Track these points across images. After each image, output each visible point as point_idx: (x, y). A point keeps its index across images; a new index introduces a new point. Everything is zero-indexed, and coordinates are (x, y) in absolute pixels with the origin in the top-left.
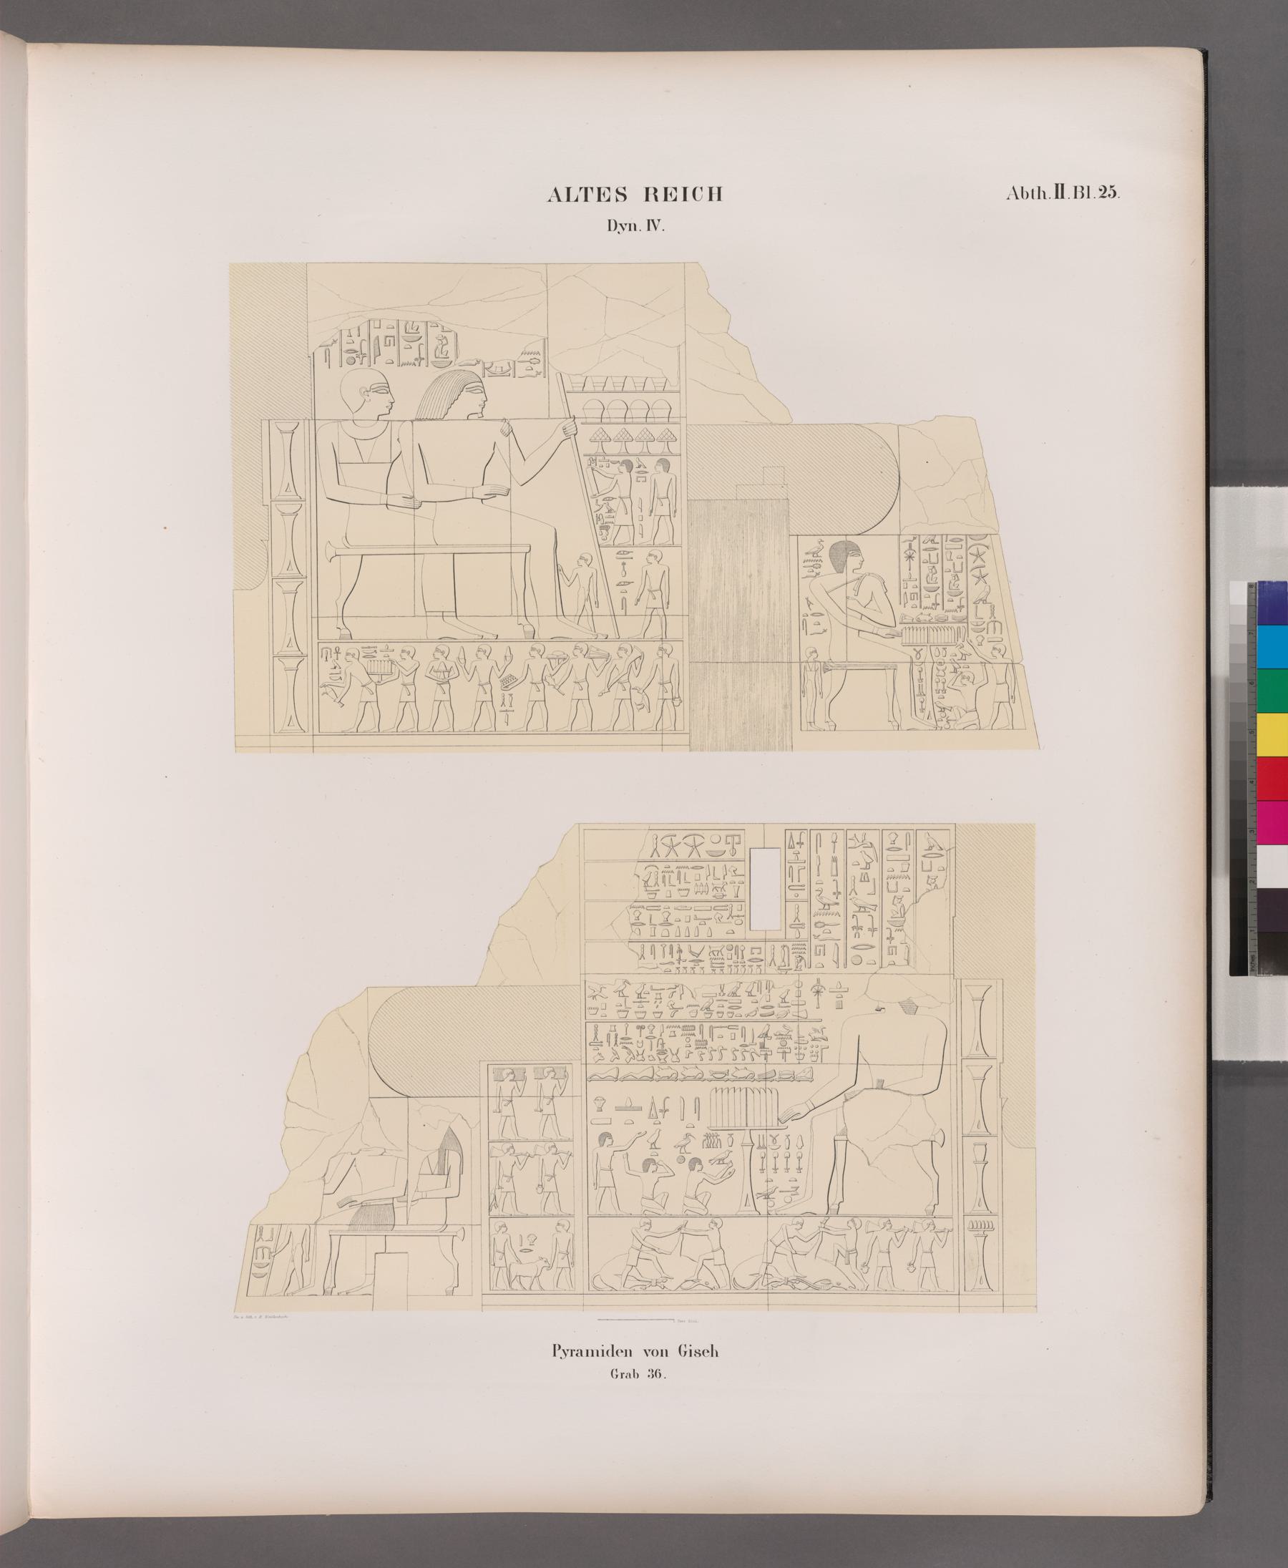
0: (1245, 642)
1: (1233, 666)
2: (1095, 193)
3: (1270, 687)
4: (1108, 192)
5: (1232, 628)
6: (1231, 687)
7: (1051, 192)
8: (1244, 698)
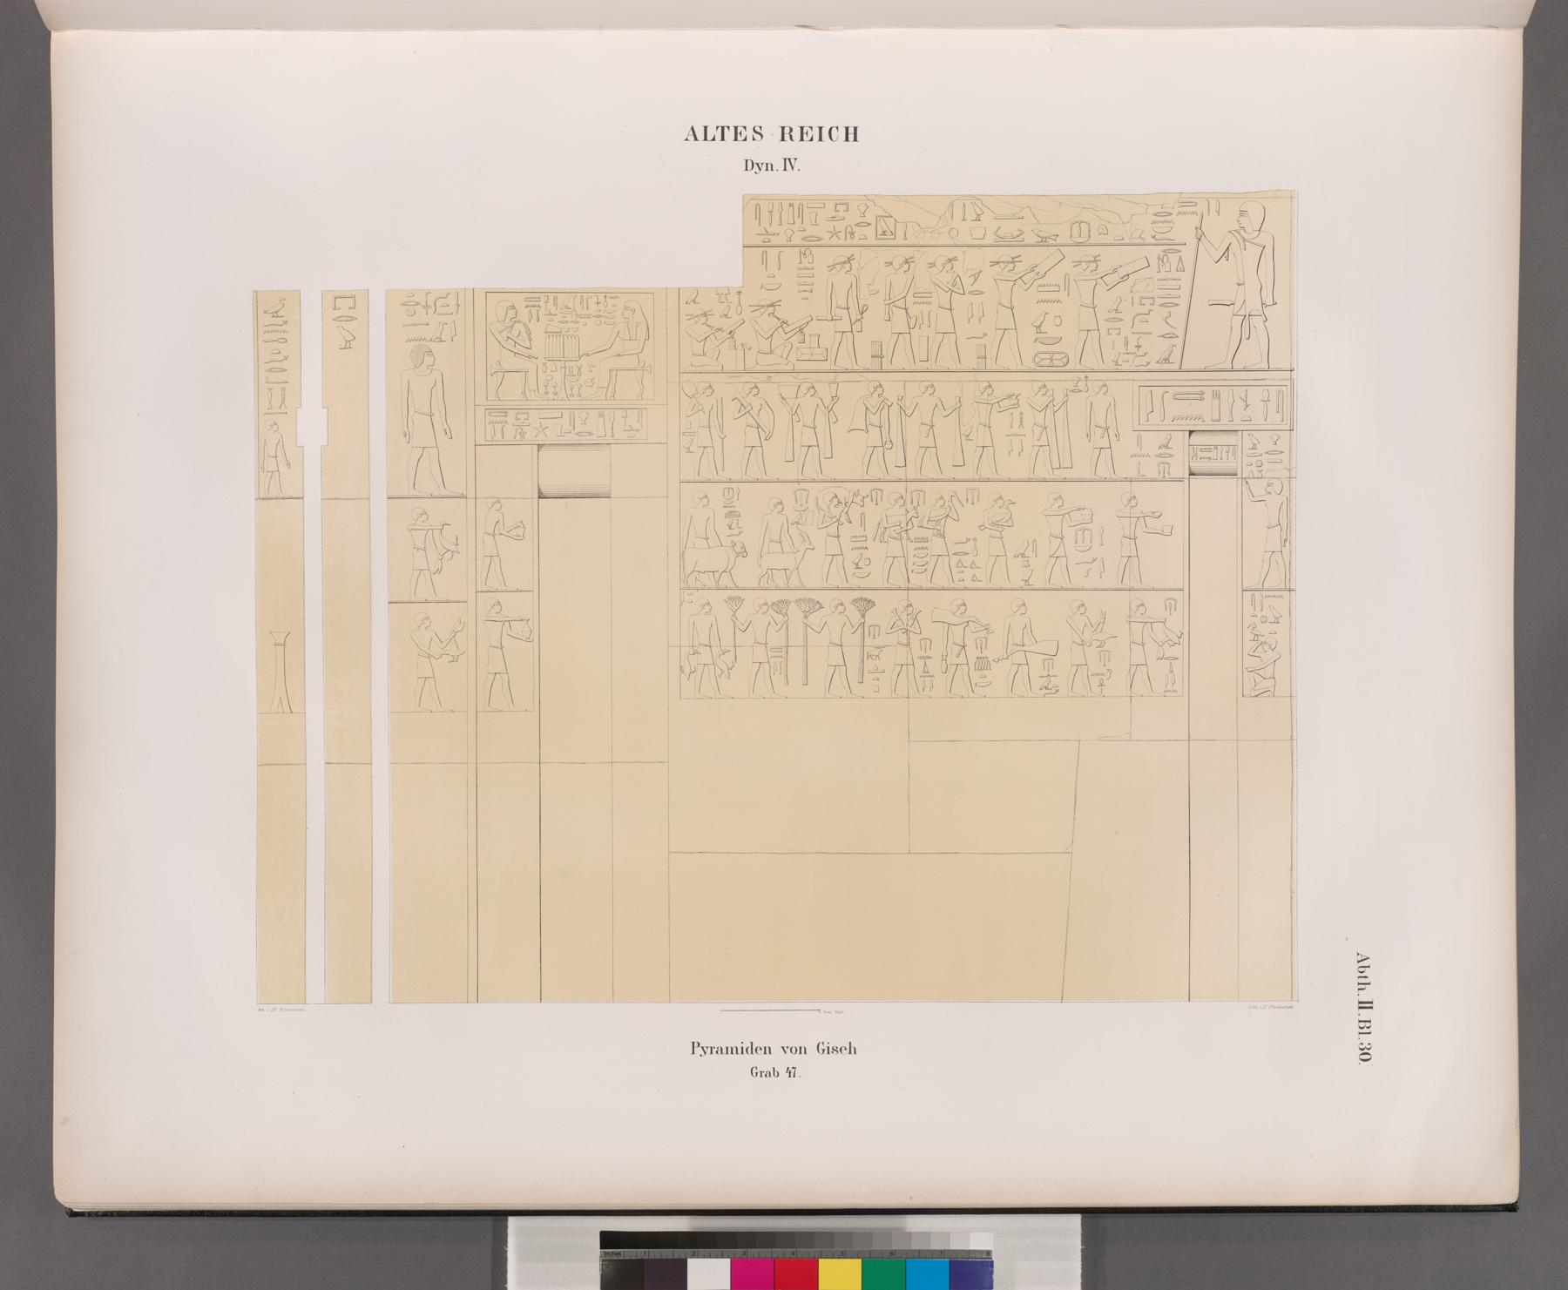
2: (1365, 1039)
3: (888, 1273)
4: (1365, 1054)
5: (947, 1235)
6: (887, 1234)
7: (1364, 996)
8: (877, 1246)
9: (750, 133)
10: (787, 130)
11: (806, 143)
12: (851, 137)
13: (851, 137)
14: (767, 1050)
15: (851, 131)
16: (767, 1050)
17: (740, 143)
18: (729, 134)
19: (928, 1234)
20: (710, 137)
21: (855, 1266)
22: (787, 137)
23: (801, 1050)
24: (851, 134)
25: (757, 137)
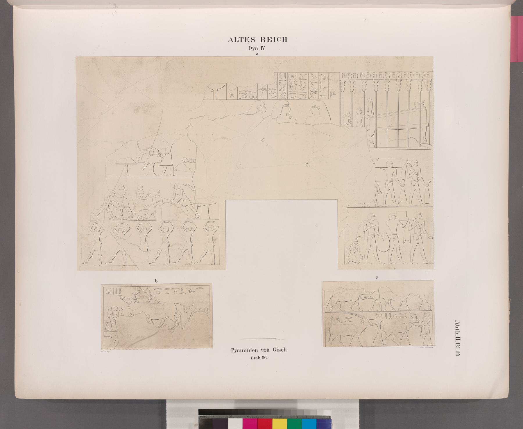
0: (311, 415)
1: (302, 411)
2: (458, 350)
5: (316, 411)
6: (296, 410)
7: (457, 336)
8: (292, 414)
9: (250, 39)
10: (263, 39)
11: (269, 43)
12: (285, 40)
13: (285, 40)
14: (256, 351)
15: (285, 39)
16: (256, 351)
17: (247, 43)
18: (243, 40)
19: (309, 411)
20: (237, 41)
21: (285, 420)
22: (263, 41)
23: (267, 350)
24: (285, 40)
25: (253, 41)
